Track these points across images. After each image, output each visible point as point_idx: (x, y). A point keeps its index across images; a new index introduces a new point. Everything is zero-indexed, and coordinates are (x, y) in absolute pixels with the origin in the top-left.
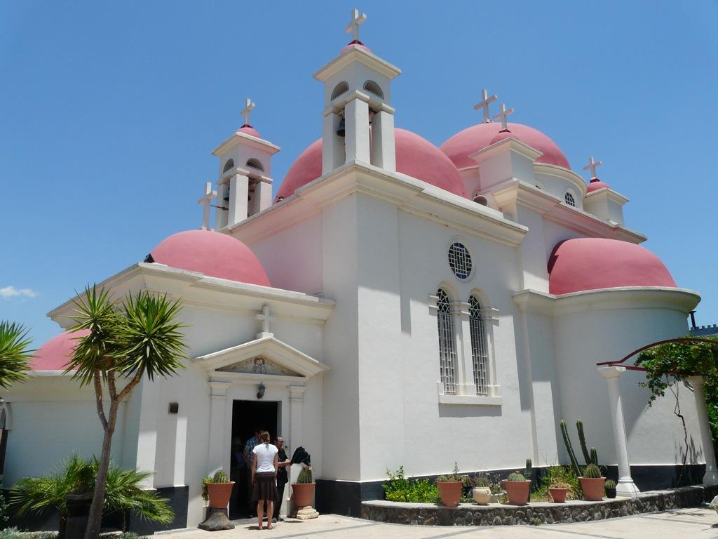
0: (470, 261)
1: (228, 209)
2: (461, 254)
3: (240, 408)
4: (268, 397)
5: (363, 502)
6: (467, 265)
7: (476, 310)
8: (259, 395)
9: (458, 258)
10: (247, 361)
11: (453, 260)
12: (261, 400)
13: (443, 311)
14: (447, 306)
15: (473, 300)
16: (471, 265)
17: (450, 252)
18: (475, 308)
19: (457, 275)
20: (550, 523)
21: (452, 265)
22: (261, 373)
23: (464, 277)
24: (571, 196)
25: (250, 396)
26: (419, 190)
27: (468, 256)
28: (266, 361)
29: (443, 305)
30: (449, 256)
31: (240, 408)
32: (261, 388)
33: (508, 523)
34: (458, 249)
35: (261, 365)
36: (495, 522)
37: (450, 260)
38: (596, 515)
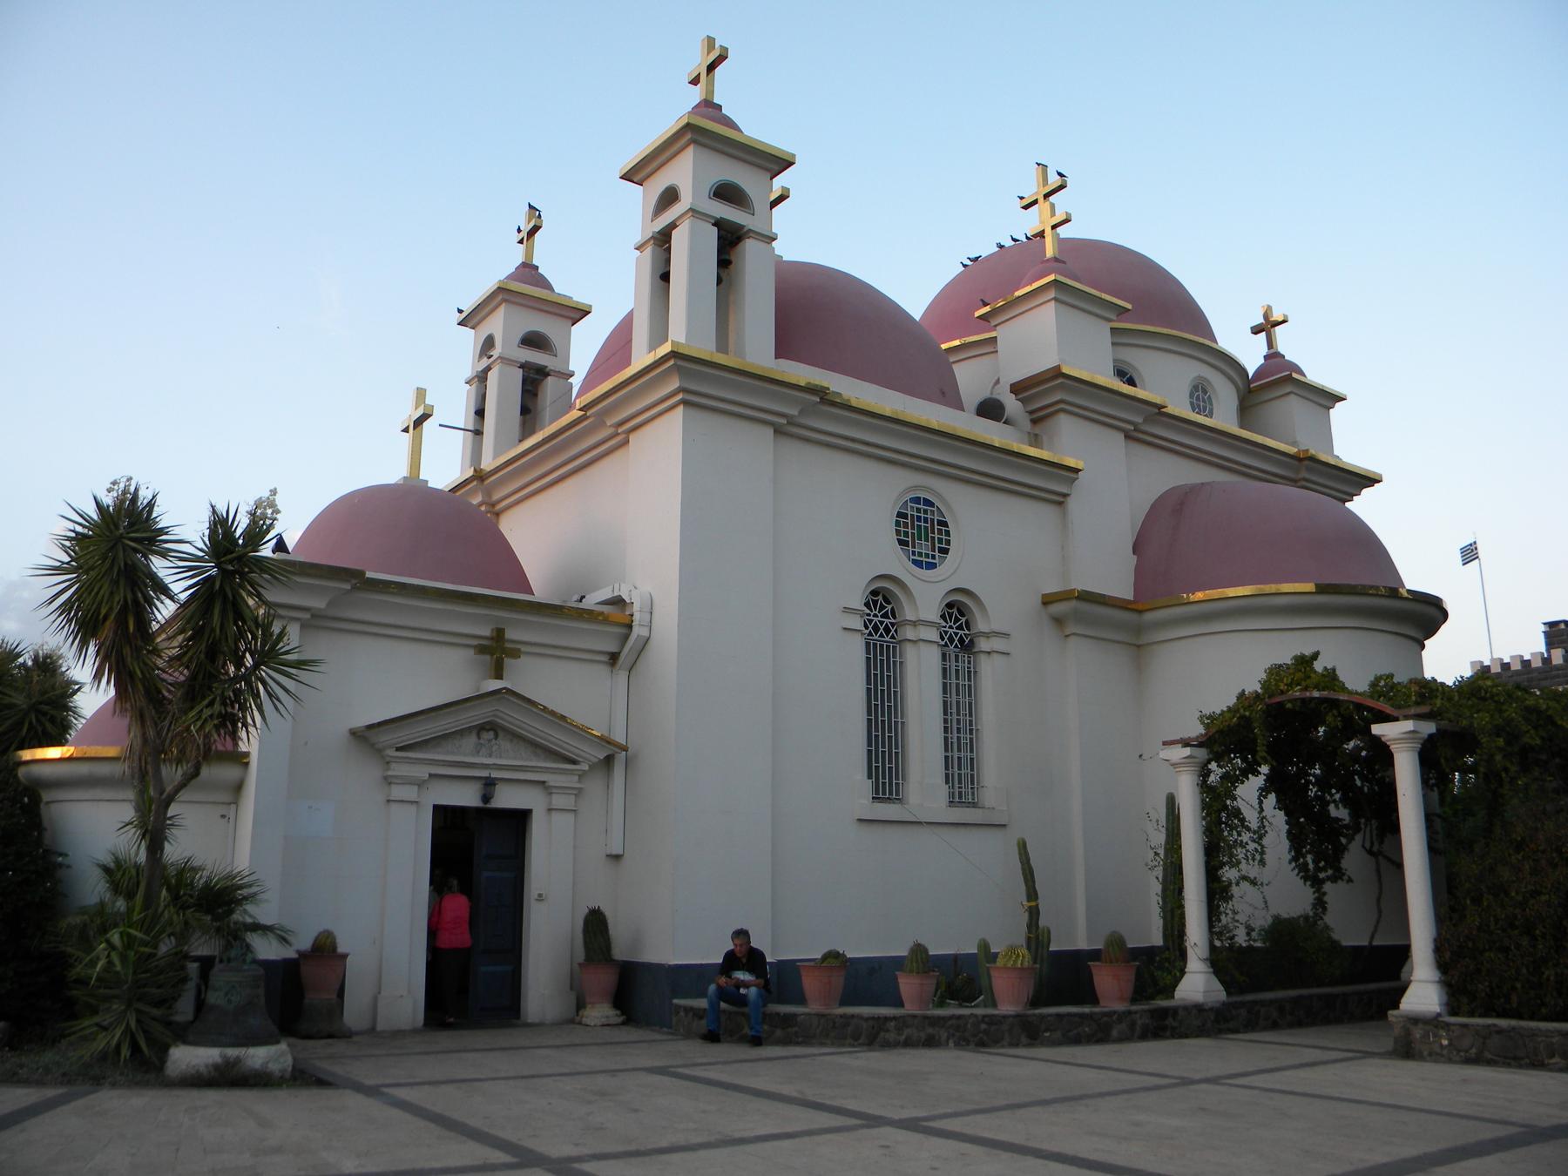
0: (948, 533)
1: (483, 433)
2: (926, 520)
3: (448, 821)
4: (506, 799)
5: (676, 1001)
6: (940, 541)
7: (961, 632)
8: (486, 798)
9: (919, 527)
10: (461, 733)
11: (906, 534)
12: (488, 806)
13: (881, 636)
14: (893, 625)
15: (957, 610)
16: (948, 542)
17: (900, 515)
18: (957, 628)
19: (915, 562)
20: (1015, 1044)
21: (901, 542)
22: (490, 756)
23: (932, 566)
24: (1205, 392)
25: (465, 796)
26: (821, 393)
27: (945, 524)
28: (501, 734)
29: (882, 623)
30: (898, 524)
31: (448, 821)
32: (489, 784)
33: (930, 1043)
34: (918, 510)
35: (490, 741)
36: (906, 1039)
37: (898, 533)
38: (1115, 1033)
